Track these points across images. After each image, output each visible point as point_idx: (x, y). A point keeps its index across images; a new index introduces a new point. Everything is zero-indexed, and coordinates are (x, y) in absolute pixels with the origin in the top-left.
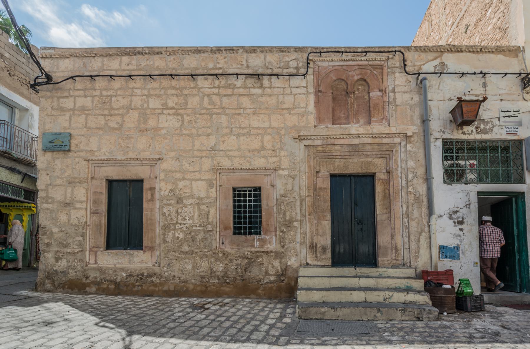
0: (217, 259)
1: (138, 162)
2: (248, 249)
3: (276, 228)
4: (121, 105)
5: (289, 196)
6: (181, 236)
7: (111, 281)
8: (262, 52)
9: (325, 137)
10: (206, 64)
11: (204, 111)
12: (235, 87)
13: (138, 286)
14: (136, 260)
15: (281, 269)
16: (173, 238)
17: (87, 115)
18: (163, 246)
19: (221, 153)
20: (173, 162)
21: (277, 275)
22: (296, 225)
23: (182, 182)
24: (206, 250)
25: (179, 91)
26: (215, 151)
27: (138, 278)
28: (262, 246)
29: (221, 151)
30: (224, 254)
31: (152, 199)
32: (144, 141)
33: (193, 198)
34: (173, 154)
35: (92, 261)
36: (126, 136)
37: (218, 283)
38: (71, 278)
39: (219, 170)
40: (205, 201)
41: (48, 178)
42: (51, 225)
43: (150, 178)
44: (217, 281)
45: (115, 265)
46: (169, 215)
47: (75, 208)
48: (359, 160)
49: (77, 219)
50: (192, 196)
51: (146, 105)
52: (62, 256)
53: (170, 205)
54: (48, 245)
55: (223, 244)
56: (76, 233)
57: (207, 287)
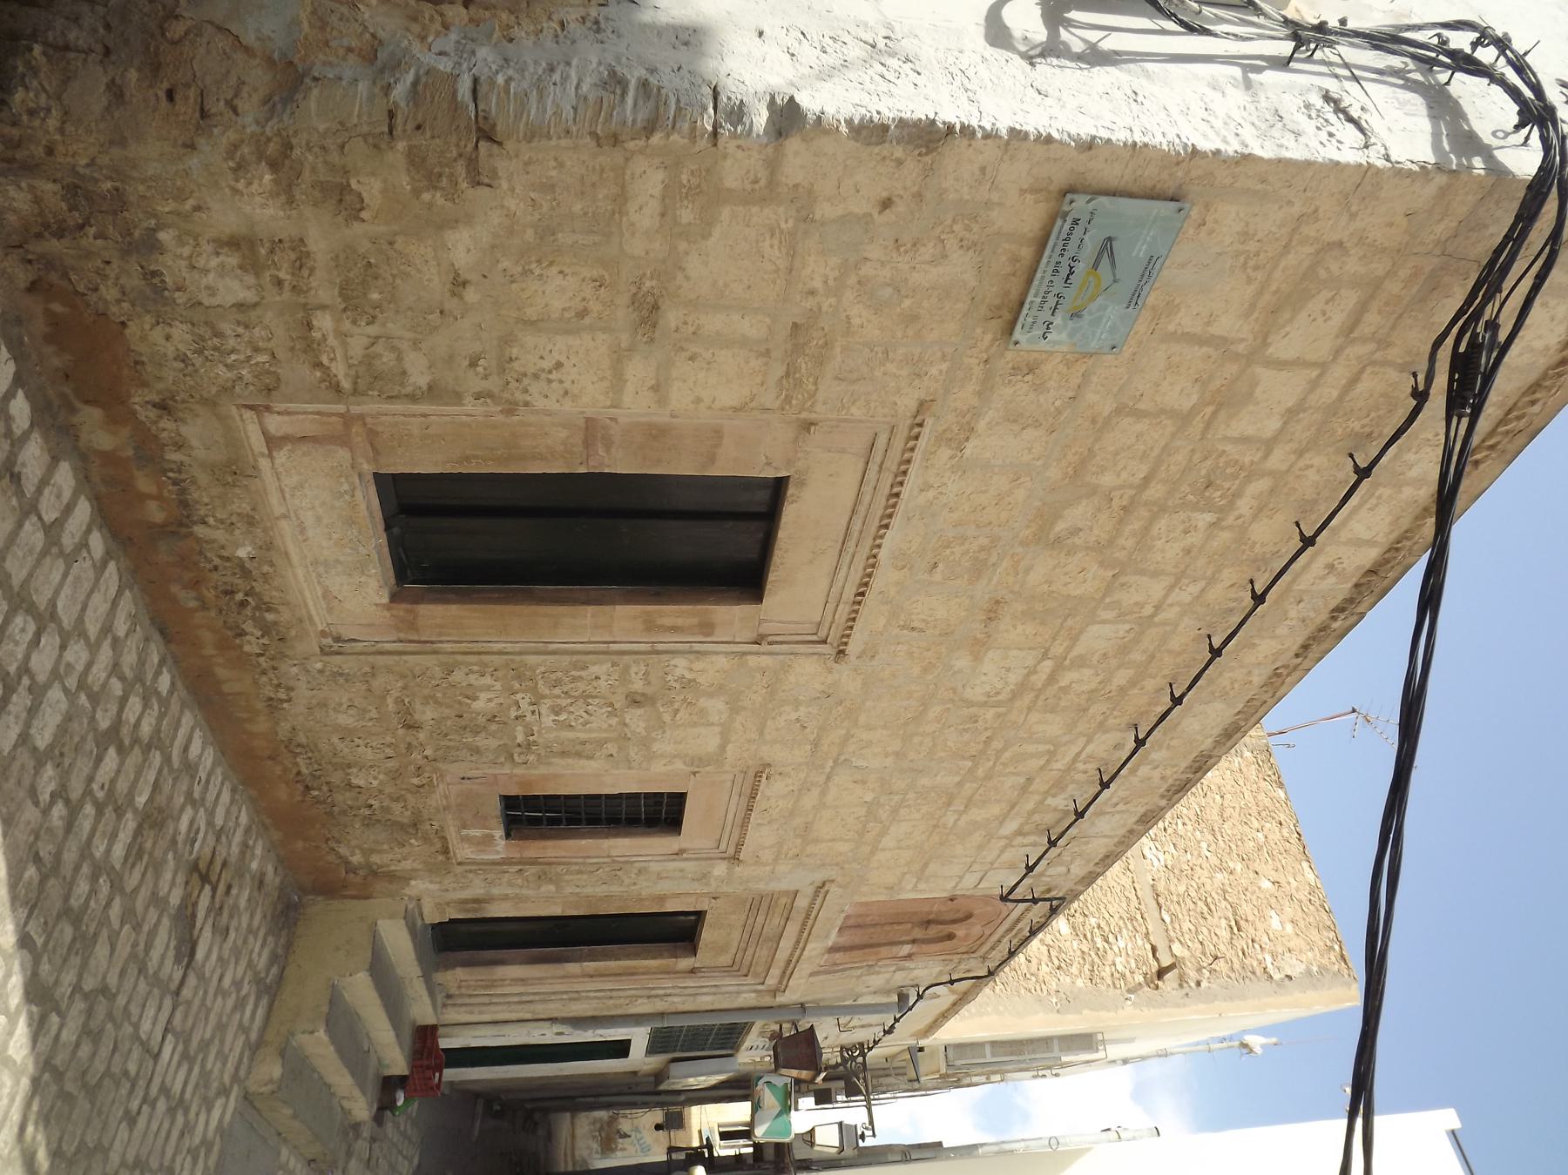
3: (534, 862)
6: (479, 705)
7: (184, 504)
8: (1131, 832)
11: (997, 744)
17: (1184, 419)
21: (368, 865)
27: (240, 596)
28: (467, 839)
29: (828, 778)
31: (650, 626)
35: (275, 424)
37: (299, 773)
38: (133, 330)
41: (859, 206)
42: (496, 218)
44: (304, 771)
45: (285, 516)
47: (619, 357)
48: (735, 944)
49: (547, 364)
52: (279, 283)
54: (341, 198)
56: (450, 359)
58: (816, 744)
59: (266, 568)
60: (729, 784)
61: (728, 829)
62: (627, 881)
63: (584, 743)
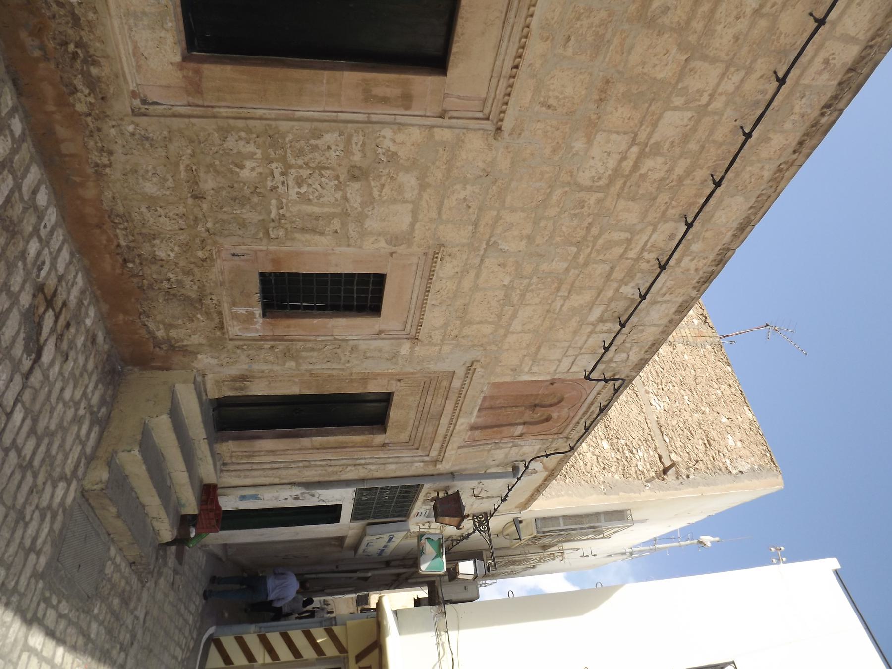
0: (186, 247)
1: (508, 64)
2: (225, 299)
3: (281, 339)
4: (719, 28)
5: (353, 356)
6: (245, 174)
9: (464, 393)
10: (704, 239)
11: (595, 231)
12: (623, 282)
13: (42, 48)
14: (144, 37)
15: (187, 346)
16: (239, 152)
18: (209, 125)
19: (477, 261)
20: (481, 164)
21: (169, 340)
22: (287, 365)
23: (413, 182)
24: (209, 225)
25: (674, 183)
26: (485, 250)
27: (71, 47)
28: (235, 317)
29: (482, 261)
30: (204, 260)
31: (369, 98)
32: (569, 91)
33: (363, 204)
34: (504, 164)
36: (608, 36)
37: (119, 246)
39: (435, 254)
40: (352, 228)
43: (446, 96)
44: (123, 243)
46: (315, 148)
48: (411, 422)
50: (369, 201)
51: (678, 101)
53: (348, 151)
55: (234, 255)
57: (99, 226)
58: (476, 225)
59: (91, 16)
60: (414, 268)
61: (412, 311)
62: (343, 359)
63: (317, 218)
